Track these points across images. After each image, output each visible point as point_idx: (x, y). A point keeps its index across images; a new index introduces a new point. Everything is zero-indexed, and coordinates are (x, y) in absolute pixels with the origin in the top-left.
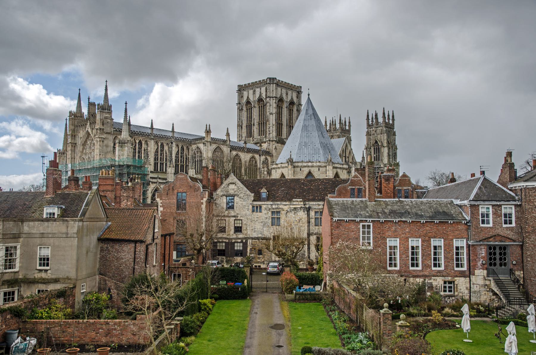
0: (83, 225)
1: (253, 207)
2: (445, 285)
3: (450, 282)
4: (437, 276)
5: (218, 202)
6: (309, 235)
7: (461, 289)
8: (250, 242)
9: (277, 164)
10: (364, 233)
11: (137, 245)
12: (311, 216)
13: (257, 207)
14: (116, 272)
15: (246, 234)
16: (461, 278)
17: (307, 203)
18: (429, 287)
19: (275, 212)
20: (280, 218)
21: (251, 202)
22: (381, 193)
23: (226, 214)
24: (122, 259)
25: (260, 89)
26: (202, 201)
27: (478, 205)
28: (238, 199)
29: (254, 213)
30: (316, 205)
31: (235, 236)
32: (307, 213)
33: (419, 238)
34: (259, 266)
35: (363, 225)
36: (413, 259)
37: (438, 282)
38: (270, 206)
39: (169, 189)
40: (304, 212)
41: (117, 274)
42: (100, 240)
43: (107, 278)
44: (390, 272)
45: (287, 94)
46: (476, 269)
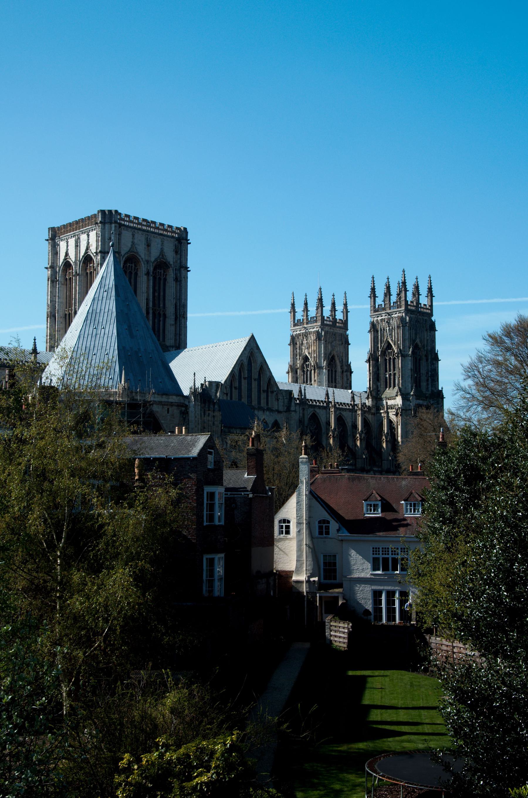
25: (88, 235)
45: (148, 245)
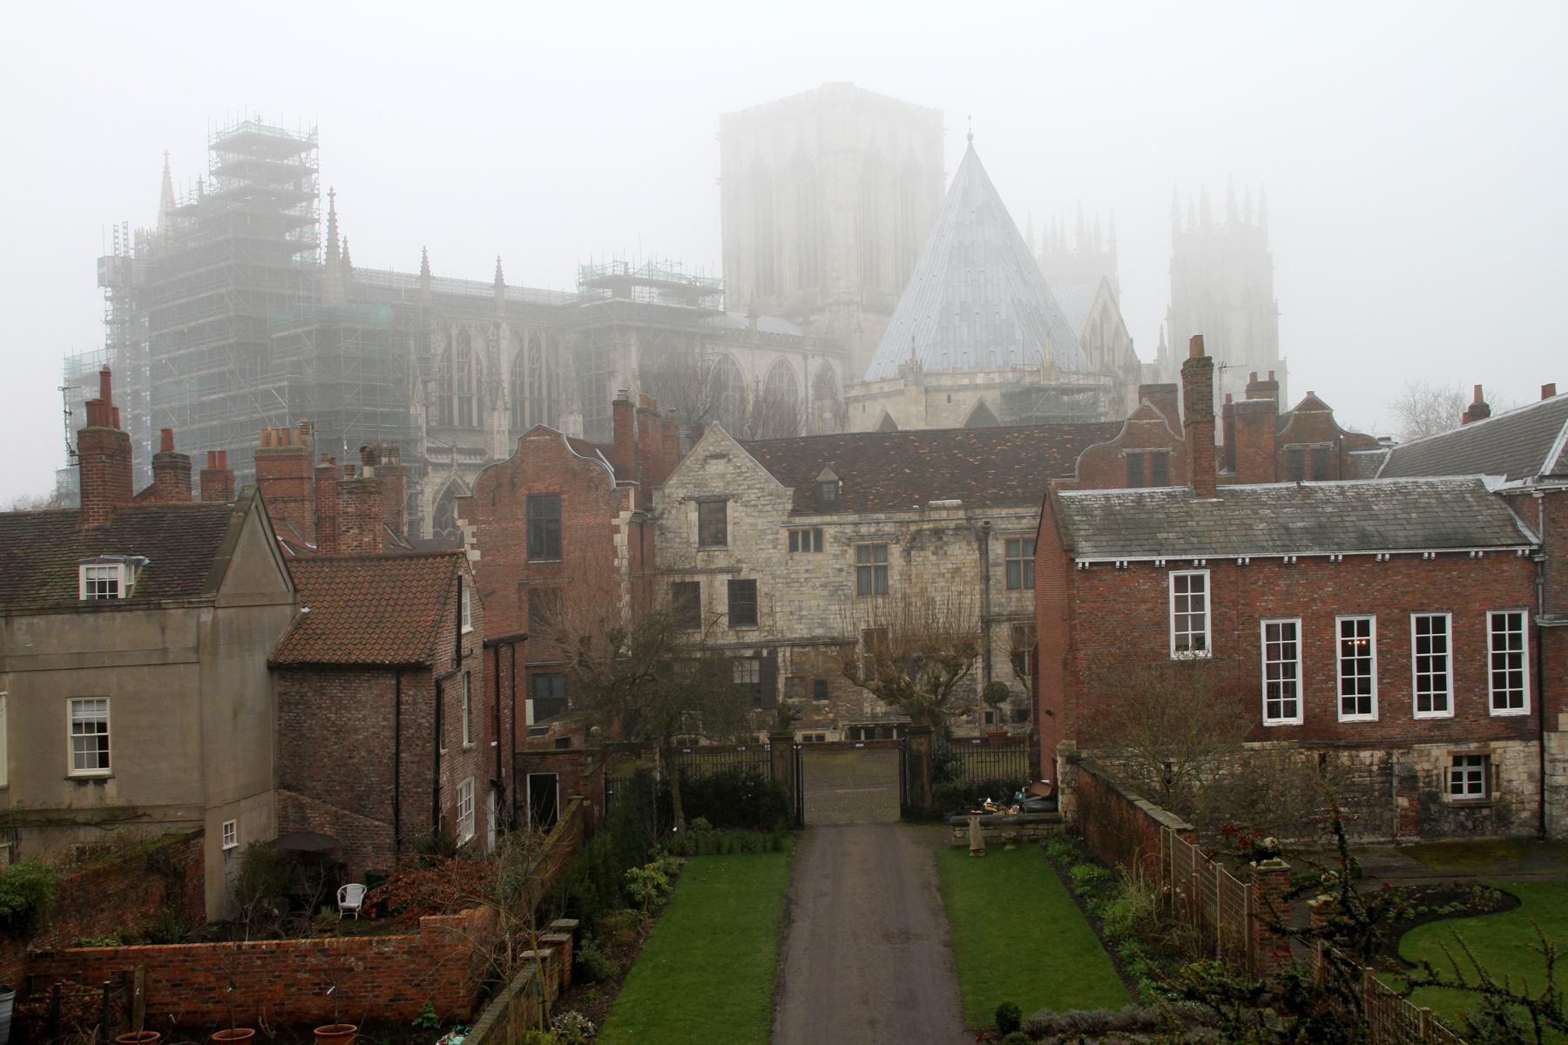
0: (215, 618)
1: (793, 535)
2: (1458, 769)
3: (1474, 760)
4: (1432, 740)
5: (668, 521)
6: (987, 622)
7: (1510, 781)
8: (784, 655)
9: (865, 384)
10: (1181, 604)
11: (404, 680)
12: (991, 556)
13: (806, 534)
14: (337, 778)
15: (770, 631)
16: (1511, 743)
17: (978, 511)
18: (1403, 780)
19: (867, 547)
20: (885, 568)
21: (785, 518)
22: (1232, 467)
23: (700, 565)
24: (356, 730)
26: (615, 522)
28: (740, 509)
29: (797, 556)
30: (1008, 518)
31: (732, 639)
32: (980, 548)
33: (1370, 612)
34: (821, 738)
35: (1177, 579)
36: (1348, 686)
37: (1438, 757)
38: (849, 530)
39: (499, 486)
40: (969, 544)
41: (340, 783)
42: (274, 668)
43: (306, 800)
46: (1562, 711)
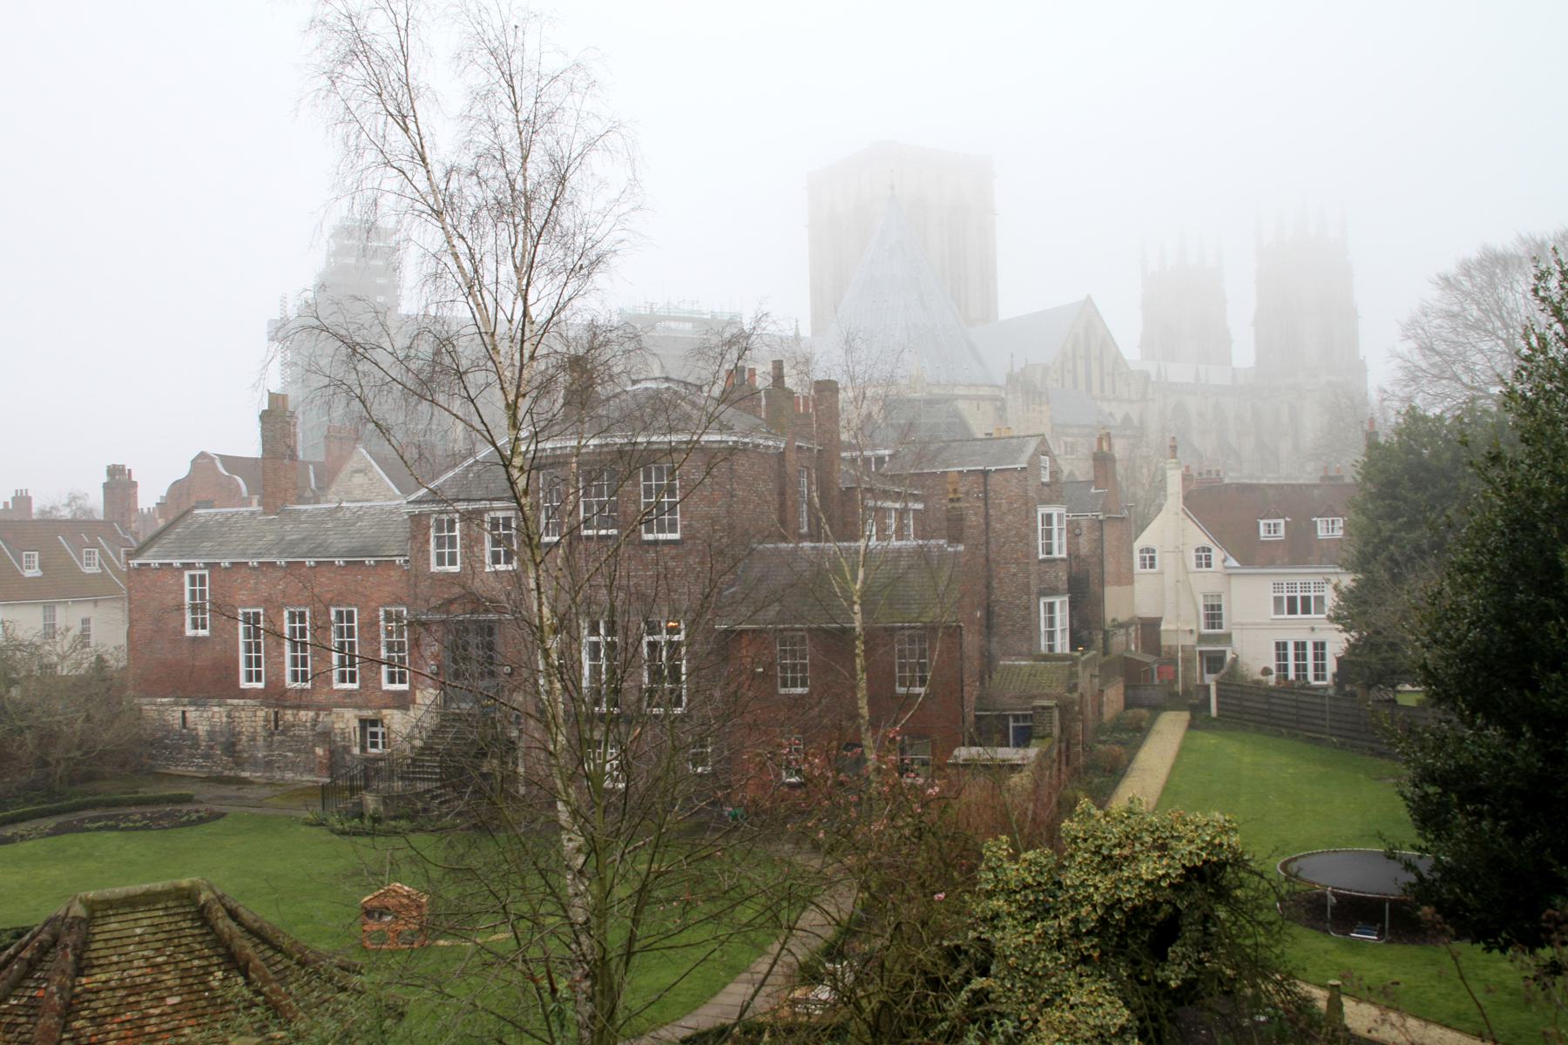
27: (428, 515)
37: (347, 721)
44: (244, 694)
